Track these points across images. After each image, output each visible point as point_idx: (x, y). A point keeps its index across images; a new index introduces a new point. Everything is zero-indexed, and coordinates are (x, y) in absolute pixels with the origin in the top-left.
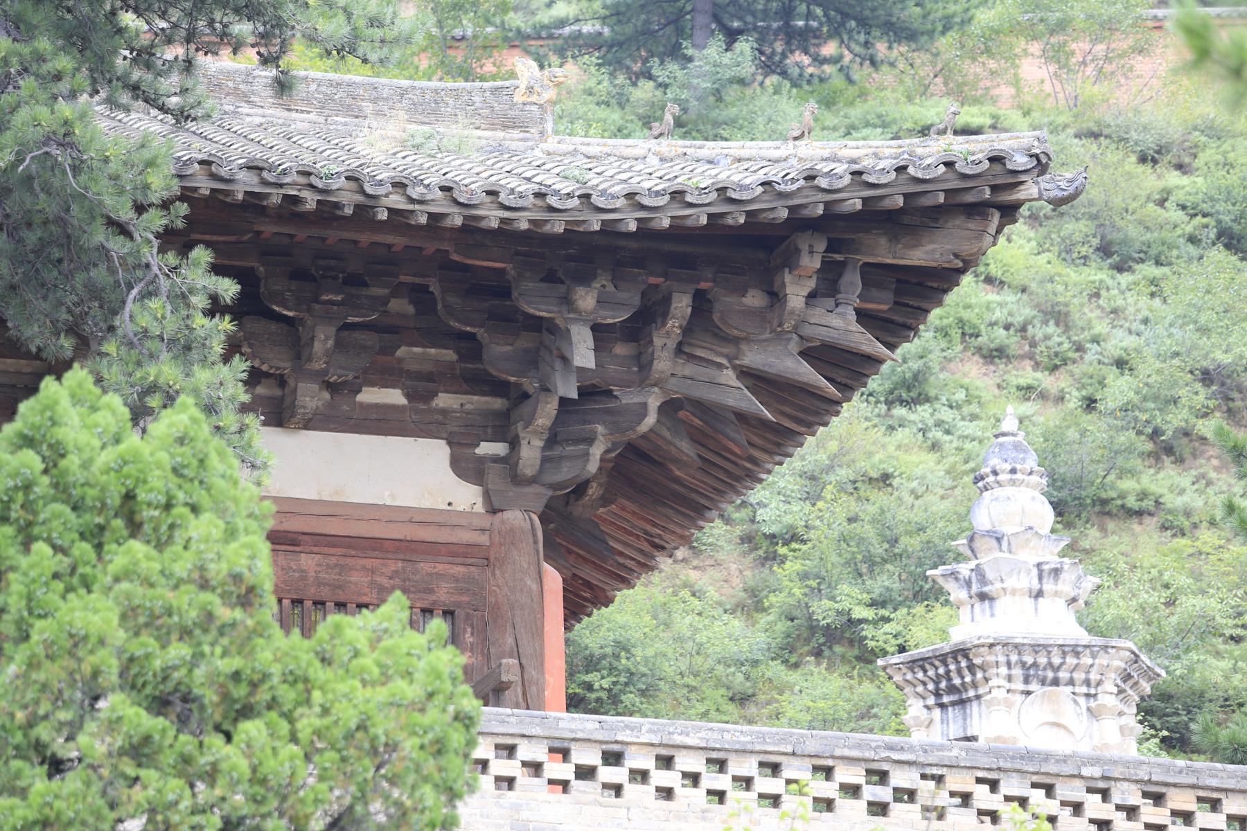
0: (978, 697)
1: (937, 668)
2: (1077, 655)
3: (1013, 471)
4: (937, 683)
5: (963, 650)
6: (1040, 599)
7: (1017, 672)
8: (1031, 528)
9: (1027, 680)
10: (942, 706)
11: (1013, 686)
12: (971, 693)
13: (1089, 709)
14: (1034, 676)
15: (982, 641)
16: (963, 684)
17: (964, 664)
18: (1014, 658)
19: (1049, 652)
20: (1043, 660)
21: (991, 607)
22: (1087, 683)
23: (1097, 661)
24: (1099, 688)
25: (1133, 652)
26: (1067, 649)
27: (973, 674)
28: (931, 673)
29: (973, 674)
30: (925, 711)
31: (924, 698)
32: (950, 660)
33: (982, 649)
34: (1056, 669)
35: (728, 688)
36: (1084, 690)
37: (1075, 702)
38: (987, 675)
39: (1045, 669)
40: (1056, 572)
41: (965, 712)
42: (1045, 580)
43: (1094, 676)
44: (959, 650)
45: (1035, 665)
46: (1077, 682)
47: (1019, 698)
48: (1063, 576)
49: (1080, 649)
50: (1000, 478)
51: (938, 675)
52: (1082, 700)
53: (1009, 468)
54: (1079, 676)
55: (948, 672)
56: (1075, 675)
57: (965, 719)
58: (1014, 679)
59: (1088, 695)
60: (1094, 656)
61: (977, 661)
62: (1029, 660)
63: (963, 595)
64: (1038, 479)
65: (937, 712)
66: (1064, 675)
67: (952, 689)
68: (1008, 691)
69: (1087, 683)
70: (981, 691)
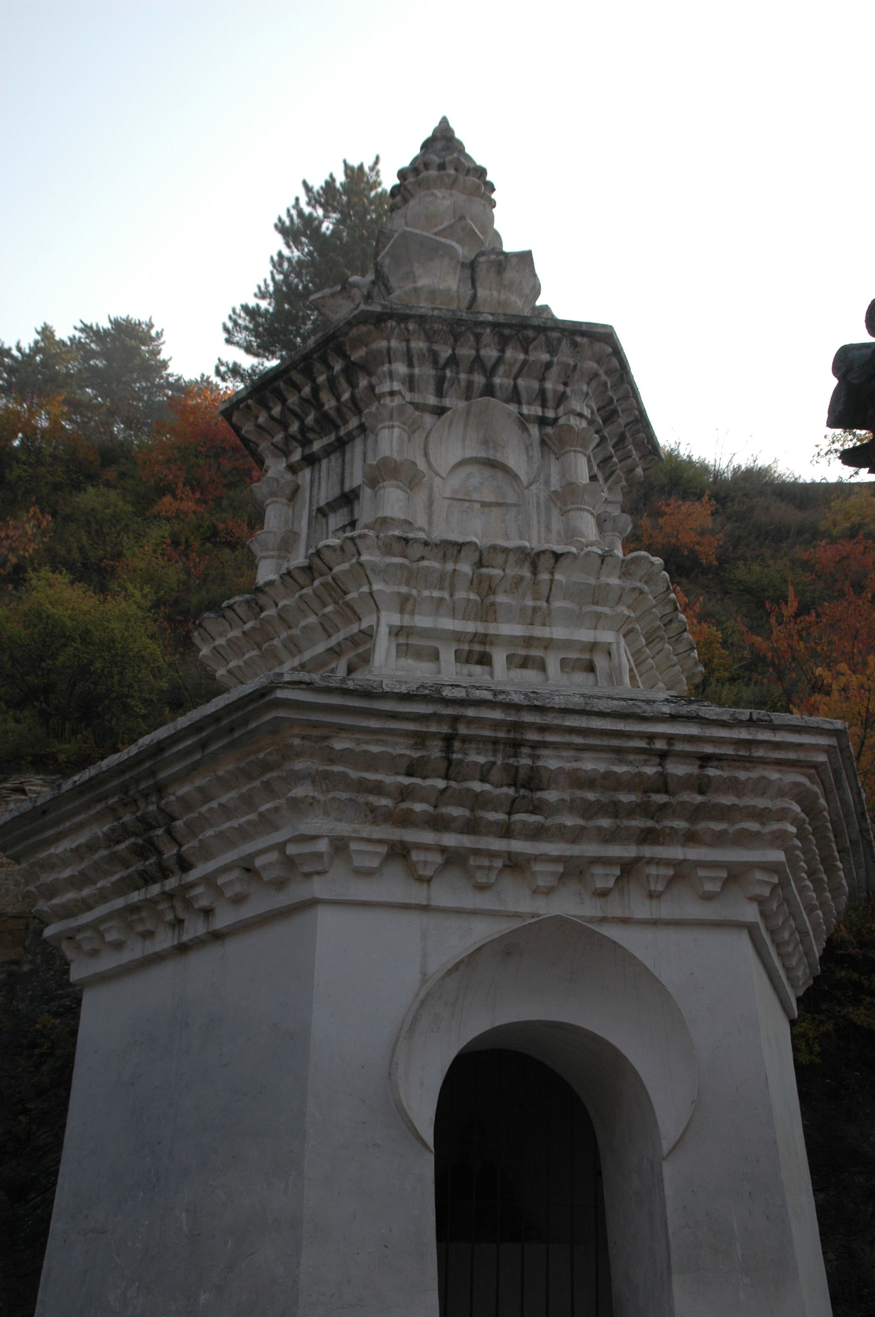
7: (425, 372)
9: (440, 393)
12: (354, 422)
13: (543, 442)
19: (478, 337)
20: (466, 352)
22: (542, 397)
24: (561, 410)
26: (507, 332)
27: (353, 385)
28: (293, 400)
31: (287, 454)
32: (318, 366)
34: (490, 373)
46: (524, 397)
47: (428, 419)
49: (530, 333)
52: (534, 430)
59: (542, 422)
60: (552, 350)
67: (327, 423)
69: (542, 397)
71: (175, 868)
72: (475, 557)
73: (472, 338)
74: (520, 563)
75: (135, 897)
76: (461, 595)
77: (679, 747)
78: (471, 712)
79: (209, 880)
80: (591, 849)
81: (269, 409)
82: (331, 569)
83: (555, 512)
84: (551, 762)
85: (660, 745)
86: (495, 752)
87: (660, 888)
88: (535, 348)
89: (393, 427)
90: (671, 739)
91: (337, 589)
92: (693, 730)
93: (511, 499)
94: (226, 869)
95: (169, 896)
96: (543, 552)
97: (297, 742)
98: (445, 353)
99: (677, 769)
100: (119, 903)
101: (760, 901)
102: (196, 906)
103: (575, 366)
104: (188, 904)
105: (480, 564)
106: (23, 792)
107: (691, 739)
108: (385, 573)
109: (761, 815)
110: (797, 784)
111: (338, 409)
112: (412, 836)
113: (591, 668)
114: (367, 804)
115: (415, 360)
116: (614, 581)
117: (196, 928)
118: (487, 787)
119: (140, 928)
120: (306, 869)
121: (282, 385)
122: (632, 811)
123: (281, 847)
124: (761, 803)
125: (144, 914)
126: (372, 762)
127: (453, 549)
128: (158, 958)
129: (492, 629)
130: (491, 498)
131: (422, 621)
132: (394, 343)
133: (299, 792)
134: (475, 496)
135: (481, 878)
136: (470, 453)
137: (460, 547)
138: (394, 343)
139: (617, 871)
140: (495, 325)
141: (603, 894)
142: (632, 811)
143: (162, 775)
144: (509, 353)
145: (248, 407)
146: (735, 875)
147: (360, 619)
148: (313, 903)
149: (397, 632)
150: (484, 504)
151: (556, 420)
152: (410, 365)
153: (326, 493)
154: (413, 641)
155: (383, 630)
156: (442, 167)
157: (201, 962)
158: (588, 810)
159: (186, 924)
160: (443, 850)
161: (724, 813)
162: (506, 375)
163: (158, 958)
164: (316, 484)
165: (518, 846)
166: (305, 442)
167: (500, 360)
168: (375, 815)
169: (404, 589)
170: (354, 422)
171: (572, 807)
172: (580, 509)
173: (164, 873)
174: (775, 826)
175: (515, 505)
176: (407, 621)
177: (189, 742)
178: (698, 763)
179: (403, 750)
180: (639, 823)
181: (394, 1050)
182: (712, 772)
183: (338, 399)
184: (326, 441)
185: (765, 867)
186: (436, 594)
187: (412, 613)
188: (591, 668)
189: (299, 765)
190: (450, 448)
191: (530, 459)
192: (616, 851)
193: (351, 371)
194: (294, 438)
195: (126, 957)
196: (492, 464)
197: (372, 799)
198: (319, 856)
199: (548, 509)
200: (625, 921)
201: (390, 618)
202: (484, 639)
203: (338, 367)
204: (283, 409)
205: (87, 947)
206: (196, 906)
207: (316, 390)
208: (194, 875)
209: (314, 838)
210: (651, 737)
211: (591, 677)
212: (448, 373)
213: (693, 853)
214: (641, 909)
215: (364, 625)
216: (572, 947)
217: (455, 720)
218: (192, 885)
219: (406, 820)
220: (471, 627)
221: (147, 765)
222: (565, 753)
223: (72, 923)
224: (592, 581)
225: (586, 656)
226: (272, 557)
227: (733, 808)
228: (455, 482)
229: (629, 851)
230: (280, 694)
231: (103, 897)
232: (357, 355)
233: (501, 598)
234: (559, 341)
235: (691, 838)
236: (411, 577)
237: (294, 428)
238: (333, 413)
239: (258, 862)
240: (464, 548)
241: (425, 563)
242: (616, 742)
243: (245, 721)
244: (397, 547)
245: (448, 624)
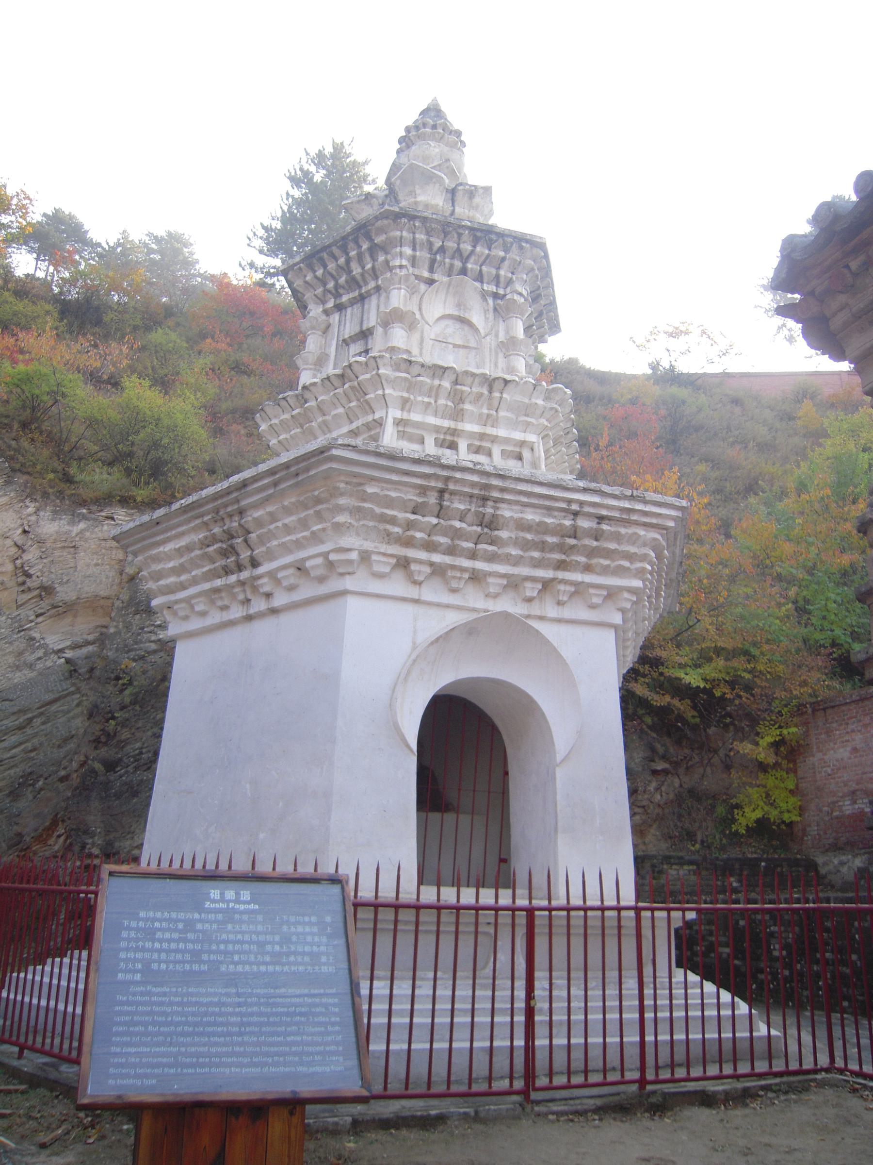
7: (423, 255)
9: (431, 270)
13: (495, 310)
19: (460, 235)
20: (451, 244)
22: (497, 279)
24: (508, 290)
26: (479, 234)
27: (374, 259)
28: (331, 266)
29: (374, 259)
31: (324, 302)
32: (351, 245)
34: (465, 260)
47: (423, 287)
49: (494, 237)
52: (490, 301)
59: (496, 296)
60: (506, 251)
67: (354, 283)
69: (497, 279)
71: (248, 565)
72: (453, 377)
73: (456, 236)
74: (481, 384)
75: (218, 583)
76: (442, 402)
77: (586, 509)
78: (458, 475)
79: (271, 574)
80: (525, 571)
81: (314, 271)
82: (357, 378)
83: (501, 355)
84: (506, 512)
85: (575, 507)
86: (471, 502)
87: (565, 599)
88: (495, 248)
89: (400, 289)
90: (581, 503)
91: (360, 391)
92: (596, 499)
93: (473, 344)
94: (284, 567)
95: (242, 583)
96: (497, 378)
97: (342, 485)
98: (438, 244)
99: (584, 523)
100: (207, 586)
101: (623, 611)
102: (261, 590)
103: (520, 262)
104: (255, 589)
105: (456, 382)
106: (113, 519)
108: (393, 382)
109: (630, 557)
110: (655, 539)
111: (362, 275)
112: (412, 553)
113: (520, 458)
114: (385, 530)
115: (418, 247)
116: (540, 402)
117: (259, 605)
118: (464, 525)
119: (220, 603)
120: (341, 570)
121: (325, 255)
122: (553, 548)
124: (633, 549)
125: (223, 594)
126: (390, 503)
127: (440, 371)
128: (231, 623)
129: (460, 426)
130: (459, 342)
131: (416, 417)
132: (405, 234)
133: (341, 518)
134: (450, 340)
135: (454, 584)
137: (445, 369)
138: (405, 234)
139: (540, 586)
140: (472, 229)
141: (529, 600)
142: (553, 548)
143: (243, 503)
144: (478, 249)
145: (300, 269)
146: (611, 594)
147: (374, 413)
148: (344, 593)
149: (398, 422)
150: (455, 346)
151: (505, 295)
152: (414, 249)
153: (350, 329)
154: (409, 430)
155: (390, 421)
156: (434, 127)
157: (263, 628)
158: (526, 546)
159: (252, 602)
160: (431, 564)
161: (609, 554)
162: (475, 263)
163: (231, 623)
164: (343, 323)
165: (480, 565)
166: (337, 295)
167: (472, 252)
169: (405, 395)
170: (372, 284)
171: (516, 542)
172: (518, 355)
173: (240, 568)
174: (639, 565)
175: (475, 348)
176: (405, 416)
177: (265, 481)
178: (597, 520)
179: (411, 496)
180: (557, 556)
181: (394, 690)
182: (605, 527)
183: (363, 268)
184: (351, 295)
186: (426, 400)
187: (409, 411)
188: (520, 458)
189: (342, 501)
190: (436, 306)
191: (487, 319)
192: (541, 573)
193: (373, 250)
194: (330, 292)
195: (209, 621)
196: (463, 321)
197: (389, 527)
198: (350, 562)
199: (497, 354)
200: (541, 618)
201: (395, 413)
202: (454, 432)
203: (365, 246)
204: (324, 272)
205: (181, 613)
206: (261, 590)
207: (348, 261)
208: (261, 570)
209: (349, 550)
210: (570, 501)
211: (519, 463)
212: (438, 258)
213: (588, 578)
214: (552, 611)
216: (512, 632)
217: (447, 479)
218: (260, 577)
219: (409, 543)
220: (446, 423)
221: (234, 495)
222: (515, 507)
223: (172, 597)
224: (526, 401)
225: (518, 450)
226: (311, 369)
227: (615, 551)
228: (438, 329)
229: (549, 574)
230: (334, 452)
231: (195, 582)
232: (379, 239)
233: (467, 406)
234: (512, 244)
235: (587, 568)
236: (410, 387)
237: (331, 285)
238: (359, 278)
239: (308, 564)
240: (447, 371)
243: (307, 469)
244: (404, 366)
245: (431, 420)
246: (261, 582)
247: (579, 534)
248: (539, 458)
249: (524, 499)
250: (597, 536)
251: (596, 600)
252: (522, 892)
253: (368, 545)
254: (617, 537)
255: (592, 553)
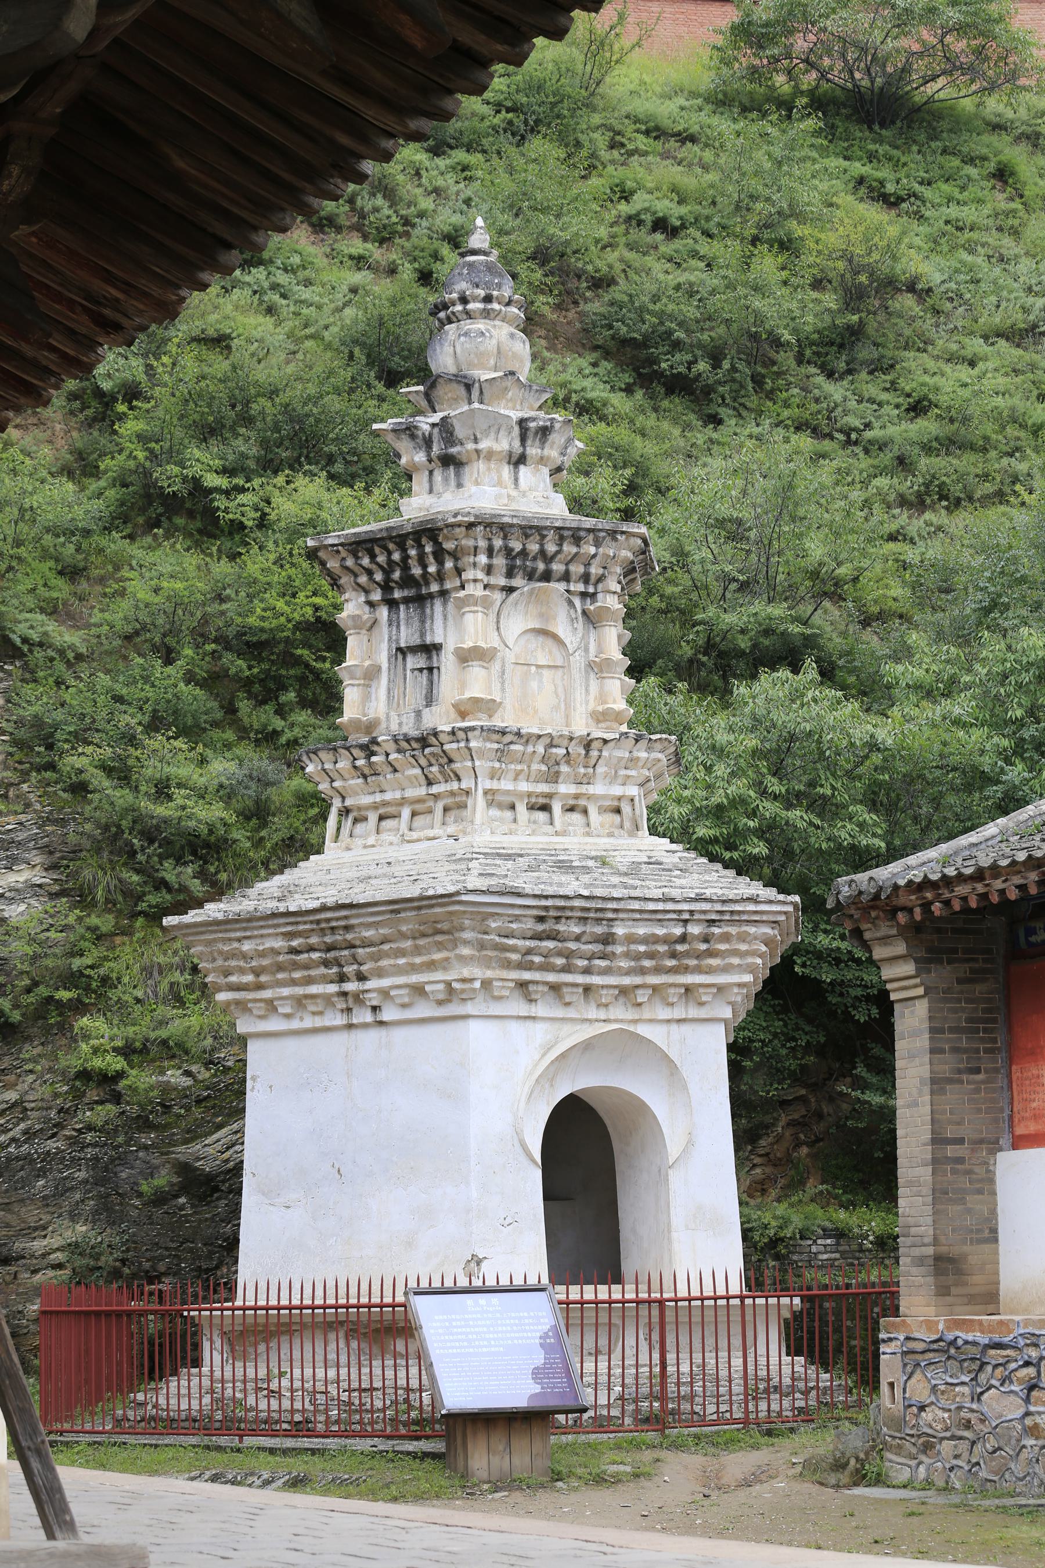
0: (444, 593)
1: (390, 553)
2: (577, 540)
3: (488, 299)
4: (387, 572)
5: (429, 530)
6: (522, 467)
7: (500, 561)
8: (512, 373)
9: (510, 574)
10: (392, 604)
11: (493, 580)
12: (434, 588)
13: (584, 613)
14: (520, 567)
15: (459, 518)
16: (425, 574)
17: (428, 549)
18: (498, 543)
19: (543, 537)
20: (534, 547)
21: (458, 475)
22: (586, 578)
23: (601, 550)
24: (600, 586)
25: (645, 541)
26: (566, 533)
27: (440, 562)
28: (381, 559)
29: (440, 562)
30: (367, 608)
31: (367, 592)
33: (457, 530)
34: (548, 559)
35: (57, 560)
36: (581, 587)
37: (571, 603)
38: (460, 564)
39: (535, 559)
40: (544, 432)
41: (423, 612)
42: (529, 442)
43: (595, 570)
44: (425, 530)
45: (524, 553)
46: (573, 577)
47: (498, 596)
48: (553, 437)
49: (582, 534)
50: (471, 306)
51: (390, 562)
52: (577, 602)
53: (482, 293)
54: (577, 569)
55: (405, 558)
56: (572, 568)
57: (423, 622)
58: (495, 571)
59: (584, 595)
60: (597, 544)
61: (449, 545)
62: (517, 546)
63: (420, 457)
64: (516, 311)
65: (383, 612)
66: (557, 567)
67: (408, 580)
68: (486, 587)
69: (586, 578)
70: (448, 585)
76: (535, 767)
79: (385, 993)
80: (638, 980)
84: (620, 930)
85: (686, 916)
90: (691, 912)
99: (695, 930)
100: (300, 991)
107: (704, 912)
113: (618, 811)
116: (644, 755)
123: (448, 984)
124: (743, 947)
131: (505, 785)
136: (531, 625)
137: (539, 737)
143: (353, 921)
145: (338, 552)
146: (721, 989)
153: (407, 636)
154: (498, 797)
155: (480, 792)
160: (546, 983)
168: (508, 965)
170: (434, 588)
171: (627, 955)
173: (342, 978)
174: (750, 960)
176: (494, 785)
179: (530, 925)
182: (716, 931)
184: (406, 593)
185: (740, 985)
188: (618, 811)
190: (517, 622)
193: (439, 555)
195: (295, 1024)
198: (474, 990)
200: (651, 1021)
208: (369, 985)
209: (472, 980)
210: (680, 912)
211: (617, 818)
212: (518, 562)
215: (464, 786)
218: (367, 991)
223: (251, 995)
225: (616, 803)
230: (464, 898)
234: (604, 538)
235: (699, 970)
236: (501, 755)
239: (428, 988)
241: (513, 747)
242: (659, 916)
243: (432, 906)
245: (524, 786)
246: (367, 996)
247: (689, 938)
248: (642, 816)
249: (638, 916)
250: (706, 940)
251: (704, 998)
252: (630, 1287)
253: (489, 974)
254: (726, 938)
255: (699, 956)
